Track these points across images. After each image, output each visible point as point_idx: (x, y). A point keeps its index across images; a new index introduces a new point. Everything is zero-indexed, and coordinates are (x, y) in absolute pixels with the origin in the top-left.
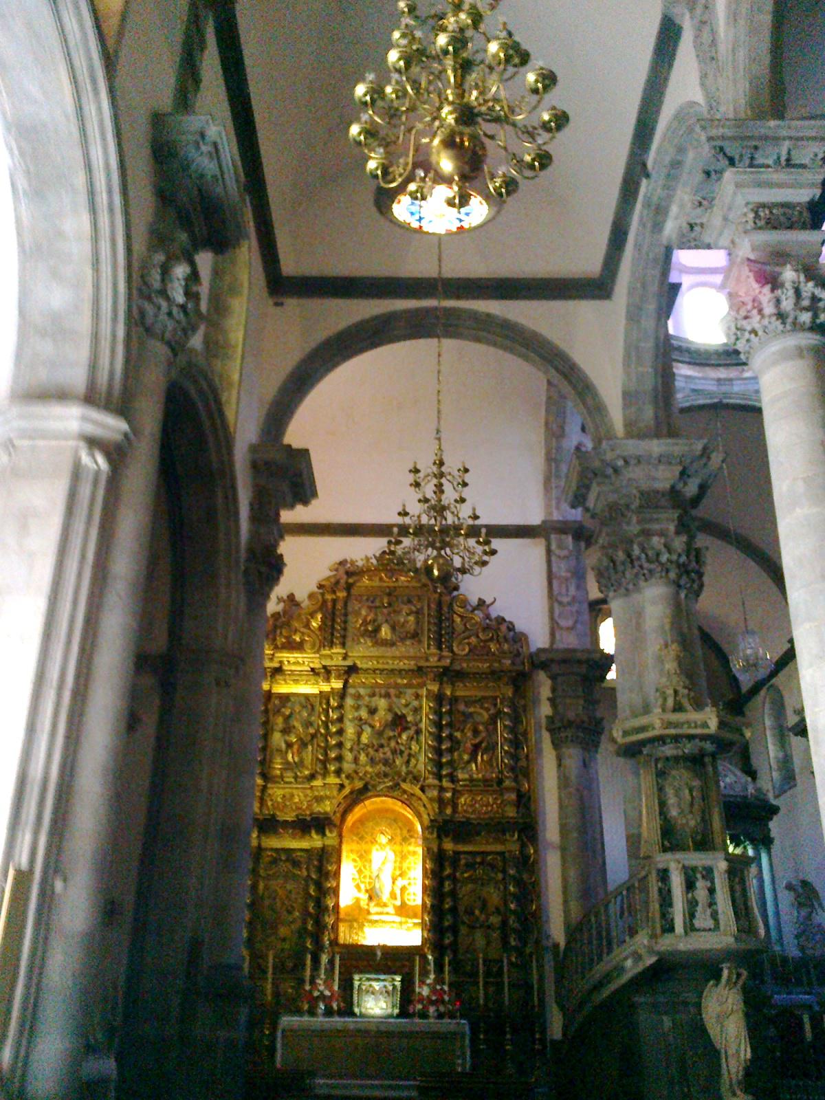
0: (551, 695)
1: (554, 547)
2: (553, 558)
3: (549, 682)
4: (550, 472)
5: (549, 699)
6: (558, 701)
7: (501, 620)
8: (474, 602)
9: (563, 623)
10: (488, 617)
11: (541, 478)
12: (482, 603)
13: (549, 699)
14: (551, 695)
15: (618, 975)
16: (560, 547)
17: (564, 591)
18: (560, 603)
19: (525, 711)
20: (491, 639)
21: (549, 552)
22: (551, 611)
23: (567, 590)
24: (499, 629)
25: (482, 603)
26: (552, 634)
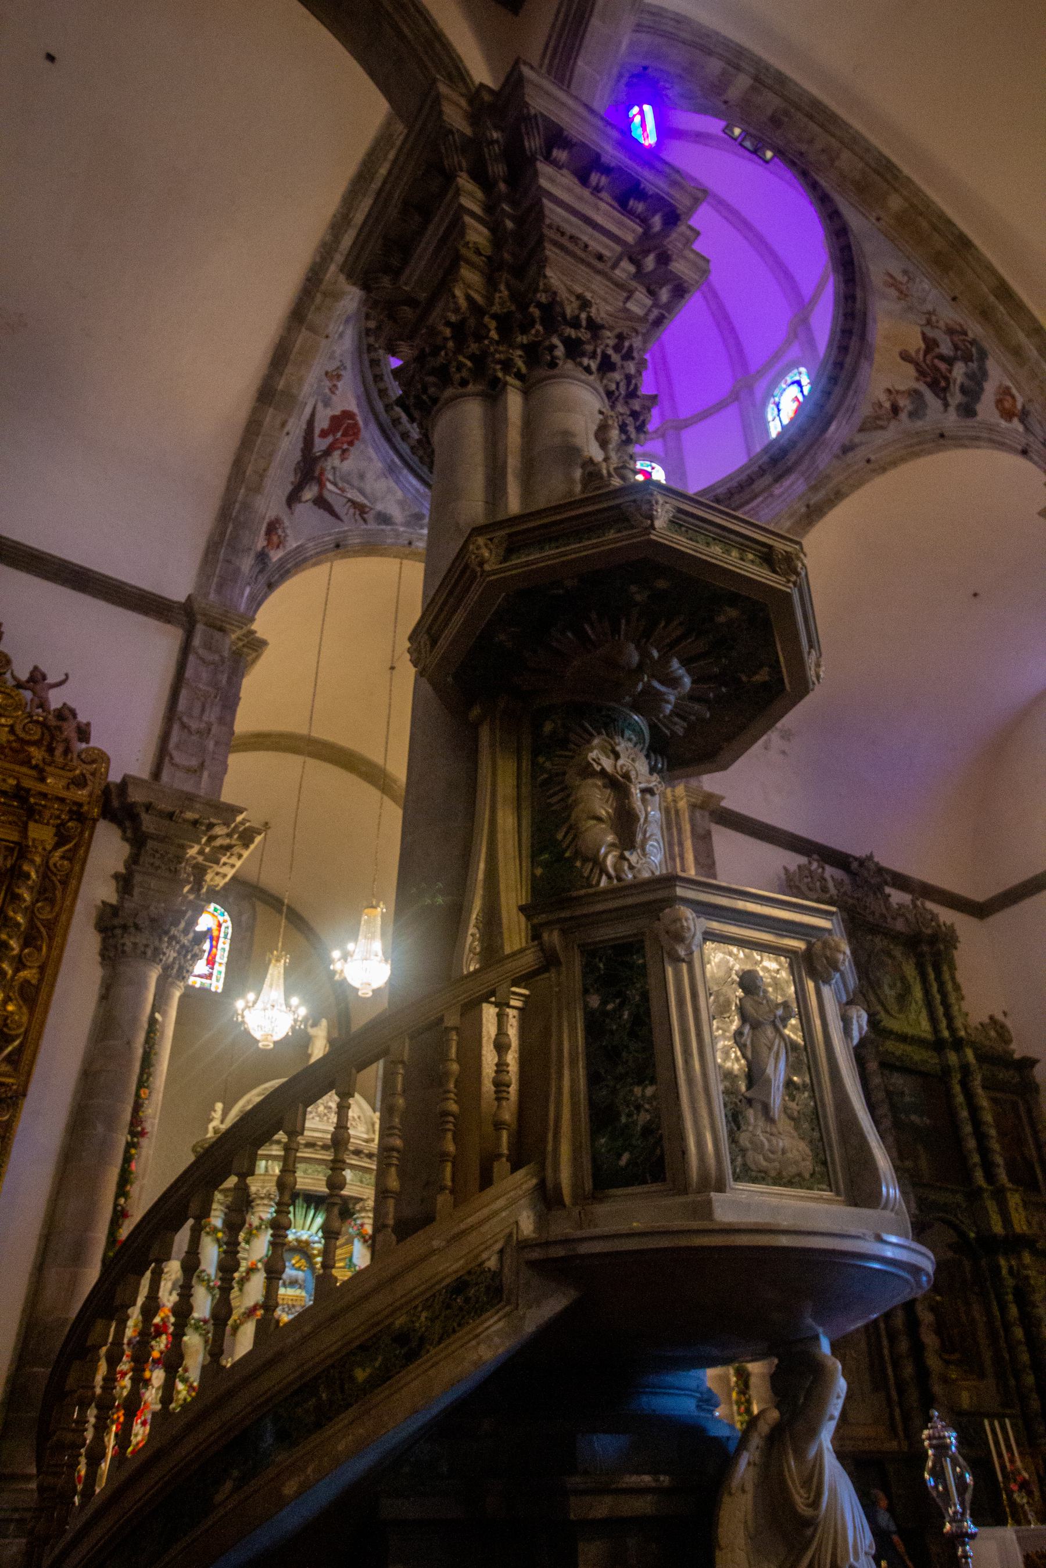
0: (122, 870)
1: (197, 642)
2: (192, 658)
3: (126, 849)
4: (223, 534)
5: (116, 876)
6: (138, 878)
7: (66, 714)
8: (24, 676)
9: (179, 757)
10: (43, 705)
11: (201, 542)
12: (37, 677)
13: (116, 876)
14: (122, 870)
15: (382, 1378)
16: (208, 646)
17: (196, 712)
18: (184, 726)
19: (64, 883)
20: (37, 743)
21: (186, 649)
22: (165, 737)
23: (203, 710)
24: (59, 728)
25: (37, 677)
26: (163, 753)
